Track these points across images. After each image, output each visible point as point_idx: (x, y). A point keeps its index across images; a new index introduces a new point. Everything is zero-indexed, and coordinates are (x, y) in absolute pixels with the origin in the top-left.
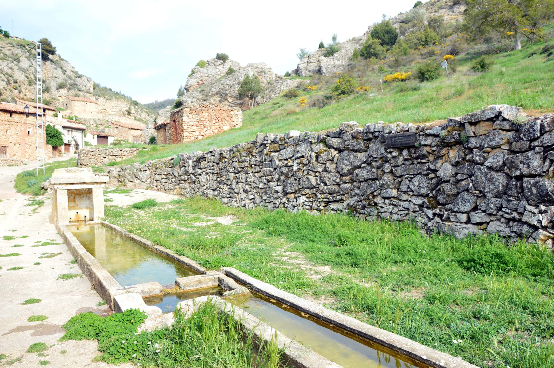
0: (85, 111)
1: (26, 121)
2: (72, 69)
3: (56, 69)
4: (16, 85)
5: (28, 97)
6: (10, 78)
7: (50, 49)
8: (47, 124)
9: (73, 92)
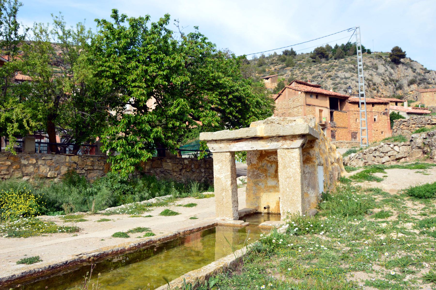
0: (433, 100)
1: (372, 110)
2: (422, 67)
3: (406, 69)
4: (375, 87)
5: (385, 95)
6: (370, 82)
7: (401, 53)
8: (391, 112)
9: (422, 85)
